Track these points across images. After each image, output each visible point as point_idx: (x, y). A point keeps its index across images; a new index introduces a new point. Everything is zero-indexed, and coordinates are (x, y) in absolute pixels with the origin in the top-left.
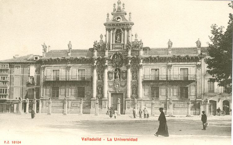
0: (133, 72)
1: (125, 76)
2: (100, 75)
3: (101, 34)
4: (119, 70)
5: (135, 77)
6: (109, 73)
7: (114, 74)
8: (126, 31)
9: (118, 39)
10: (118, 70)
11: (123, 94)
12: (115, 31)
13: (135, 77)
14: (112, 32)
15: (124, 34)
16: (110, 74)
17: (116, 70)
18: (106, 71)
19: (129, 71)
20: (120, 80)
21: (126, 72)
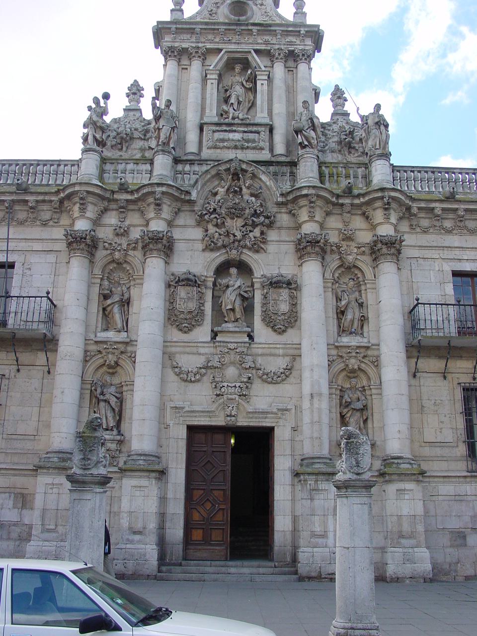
0: (333, 285)
1: (284, 307)
2: (116, 298)
3: (135, 81)
4: (244, 269)
5: (349, 316)
6: (175, 283)
7: (209, 295)
8: (279, 70)
9: (233, 100)
10: (233, 271)
11: (271, 430)
12: (215, 62)
13: (349, 316)
14: (196, 64)
15: (270, 79)
16: (182, 292)
17: (222, 269)
18: (154, 272)
19: (312, 275)
20: (251, 337)
21: (291, 285)
